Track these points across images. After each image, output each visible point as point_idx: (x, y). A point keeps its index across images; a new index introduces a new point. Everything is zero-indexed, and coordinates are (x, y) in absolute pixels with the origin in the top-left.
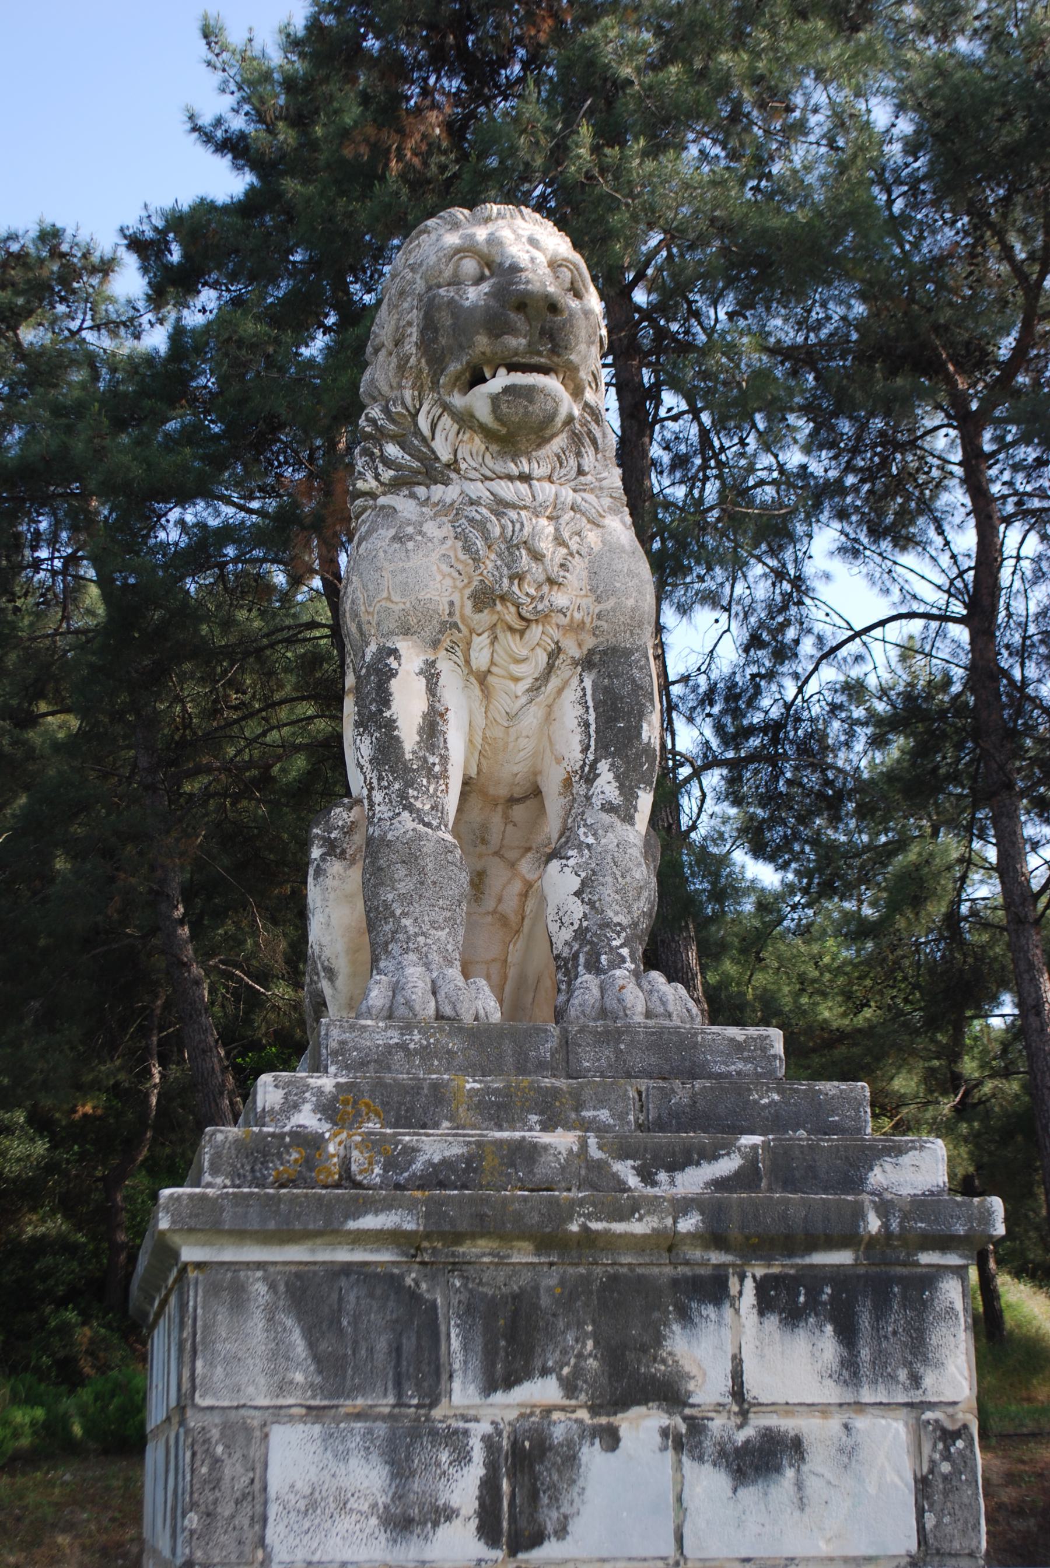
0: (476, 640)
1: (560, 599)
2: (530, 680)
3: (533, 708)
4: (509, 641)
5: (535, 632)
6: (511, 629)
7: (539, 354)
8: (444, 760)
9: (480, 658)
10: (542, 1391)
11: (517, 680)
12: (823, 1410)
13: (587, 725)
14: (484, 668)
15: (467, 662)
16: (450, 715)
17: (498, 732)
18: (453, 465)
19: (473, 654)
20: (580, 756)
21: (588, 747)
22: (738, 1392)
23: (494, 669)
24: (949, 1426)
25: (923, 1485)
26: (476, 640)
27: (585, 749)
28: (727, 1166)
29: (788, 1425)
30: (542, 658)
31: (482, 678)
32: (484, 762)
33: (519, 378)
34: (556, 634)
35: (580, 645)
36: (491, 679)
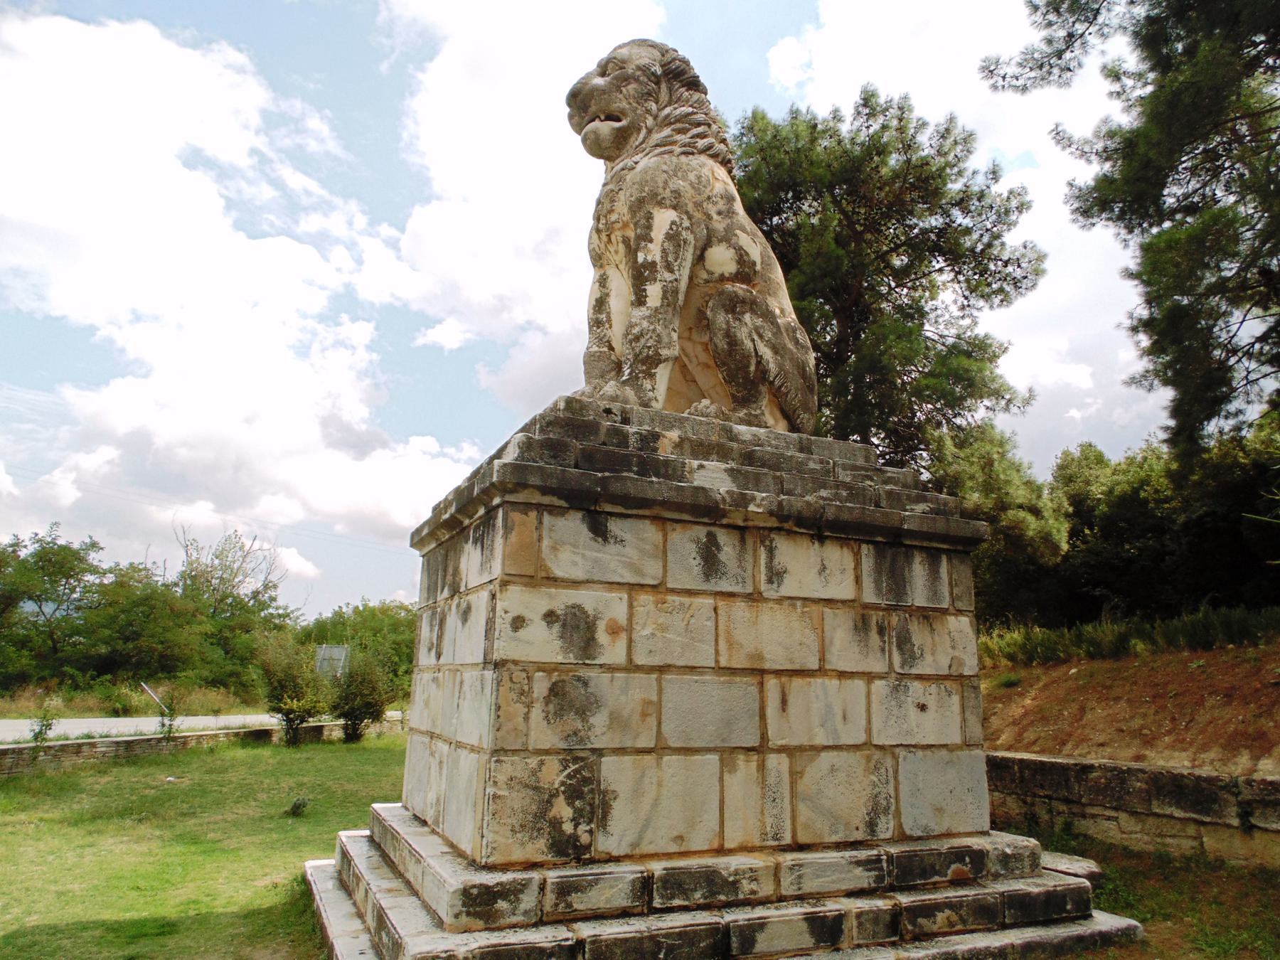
1: (613, 217)
5: (613, 237)
8: (608, 314)
16: (613, 294)
30: (621, 247)
34: (618, 233)
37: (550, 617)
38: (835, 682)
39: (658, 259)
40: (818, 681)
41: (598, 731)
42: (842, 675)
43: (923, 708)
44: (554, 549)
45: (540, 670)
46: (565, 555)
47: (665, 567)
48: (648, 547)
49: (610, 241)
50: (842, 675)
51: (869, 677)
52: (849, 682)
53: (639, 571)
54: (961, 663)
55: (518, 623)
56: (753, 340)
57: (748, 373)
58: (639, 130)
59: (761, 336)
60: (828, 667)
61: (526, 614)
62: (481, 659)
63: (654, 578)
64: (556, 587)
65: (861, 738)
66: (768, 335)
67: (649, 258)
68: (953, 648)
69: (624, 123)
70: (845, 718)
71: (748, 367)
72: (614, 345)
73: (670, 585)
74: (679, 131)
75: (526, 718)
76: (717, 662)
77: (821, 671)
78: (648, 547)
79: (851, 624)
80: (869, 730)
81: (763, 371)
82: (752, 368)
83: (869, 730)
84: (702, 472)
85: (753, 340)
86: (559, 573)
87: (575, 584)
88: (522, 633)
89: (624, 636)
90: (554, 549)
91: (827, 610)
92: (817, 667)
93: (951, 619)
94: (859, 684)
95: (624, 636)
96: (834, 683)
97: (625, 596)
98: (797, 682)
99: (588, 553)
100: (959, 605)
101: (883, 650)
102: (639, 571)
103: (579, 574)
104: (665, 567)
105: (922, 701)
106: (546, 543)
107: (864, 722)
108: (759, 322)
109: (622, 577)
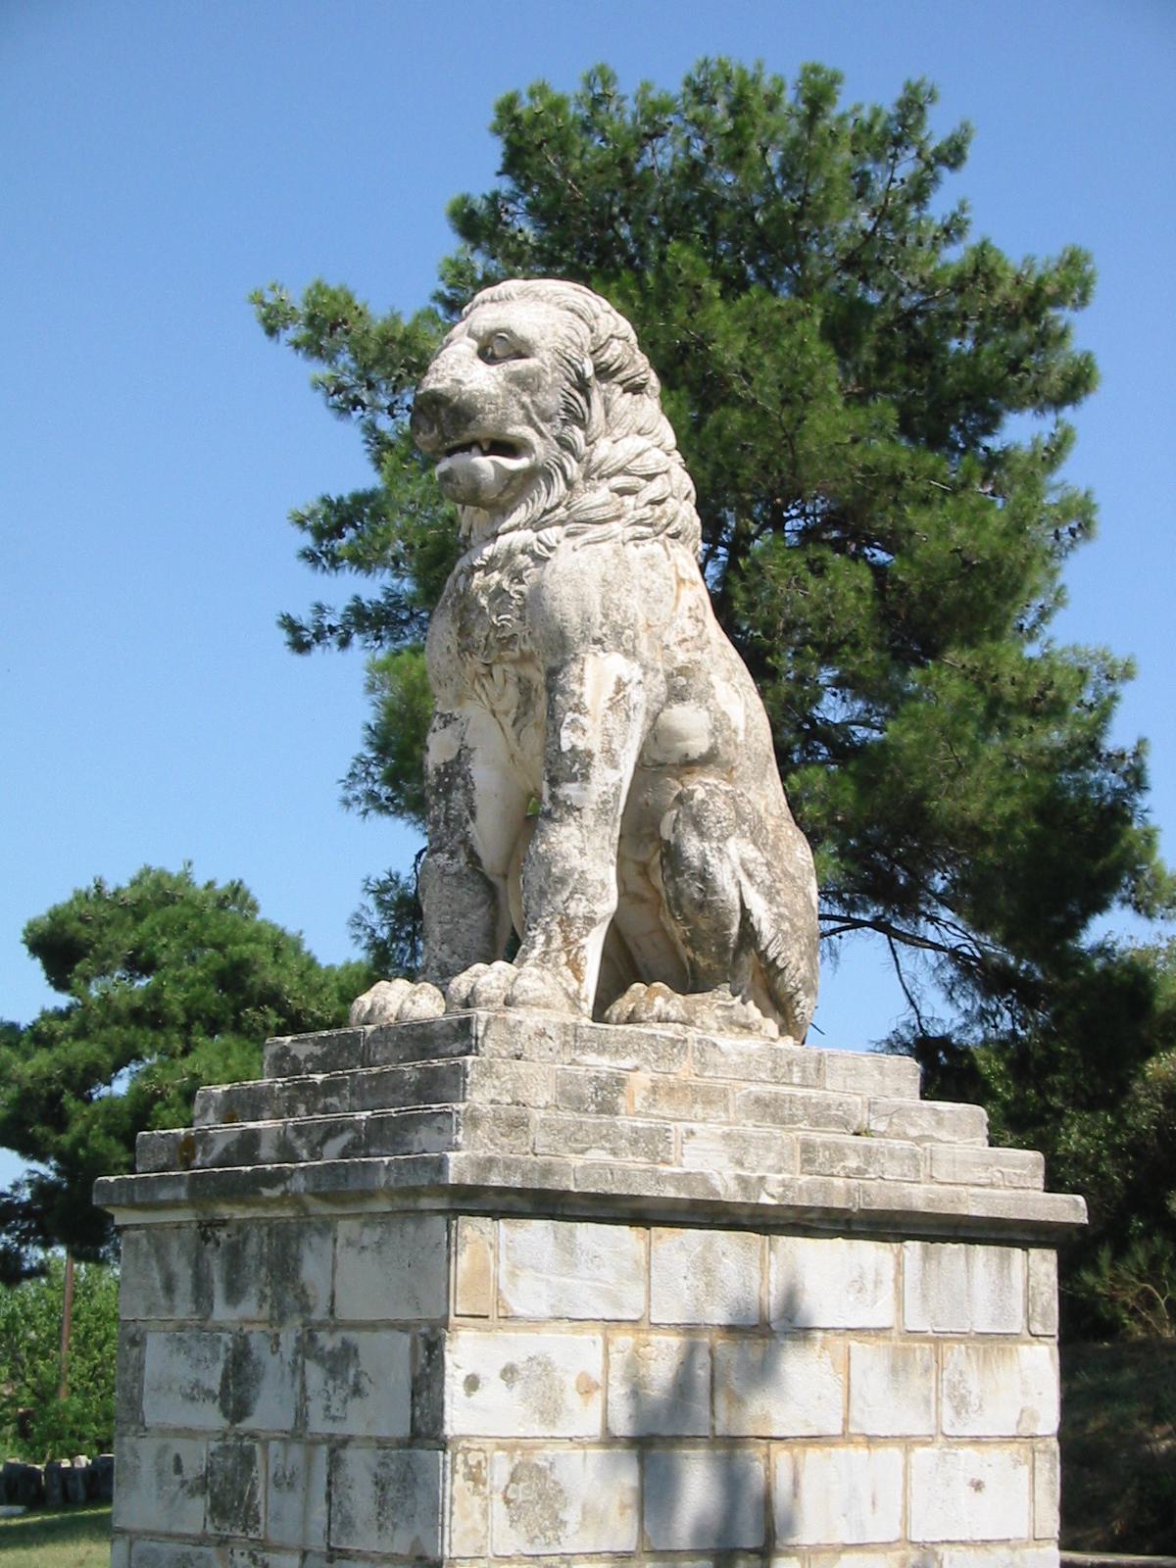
5: (497, 671)
10: (249, 1307)
12: (373, 1326)
16: (478, 755)
22: (332, 1312)
24: (433, 1339)
25: (415, 1381)
28: (346, 1137)
29: (353, 1336)
30: (512, 693)
34: (509, 668)
37: (509, 1373)
38: (863, 1451)
40: (841, 1451)
41: (571, 1528)
42: (871, 1440)
43: (978, 1486)
44: (513, 1275)
45: (499, 1447)
46: (527, 1281)
47: (649, 1291)
48: (625, 1264)
50: (871, 1440)
51: (907, 1442)
52: (881, 1451)
53: (617, 1303)
54: (1035, 1419)
55: (472, 1383)
56: (739, 884)
57: (727, 937)
58: (549, 477)
59: (750, 876)
60: (852, 1430)
61: (482, 1372)
62: (403, 1430)
63: (635, 1311)
64: (516, 1330)
65: (894, 1533)
66: (762, 873)
68: (1024, 1393)
70: (874, 1503)
71: (727, 928)
72: (481, 851)
73: (653, 1320)
74: (622, 492)
75: (485, 1514)
76: (713, 1428)
77: (845, 1438)
78: (625, 1264)
79: (886, 1362)
80: (905, 1522)
81: (749, 934)
82: (735, 930)
83: (905, 1522)
84: (692, 1142)
85: (739, 884)
86: (519, 1310)
87: (534, 1323)
88: (477, 1395)
89: (598, 1396)
90: (513, 1275)
91: (853, 1344)
92: (839, 1432)
93: (1024, 1349)
94: (895, 1453)
95: (598, 1396)
96: (861, 1452)
97: (599, 1338)
98: (813, 1454)
99: (552, 1278)
100: (1037, 1329)
101: (927, 1402)
102: (617, 1303)
103: (543, 1310)
104: (649, 1291)
105: (978, 1477)
106: (504, 1266)
107: (899, 1509)
108: (751, 852)
109: (596, 1310)
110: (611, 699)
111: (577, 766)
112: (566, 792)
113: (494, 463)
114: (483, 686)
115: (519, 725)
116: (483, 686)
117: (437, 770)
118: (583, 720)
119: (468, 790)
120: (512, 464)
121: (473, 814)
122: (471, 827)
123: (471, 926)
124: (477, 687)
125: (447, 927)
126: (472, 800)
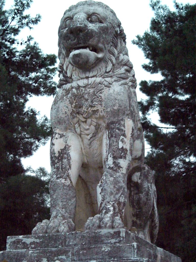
0: (76, 125)
2: (91, 134)
3: (95, 142)
4: (83, 125)
5: (89, 121)
6: (83, 122)
7: (80, 44)
9: (78, 130)
11: (88, 135)
13: (107, 144)
14: (79, 133)
15: (76, 132)
16: (72, 148)
17: (88, 150)
18: (71, 78)
19: (76, 130)
20: (106, 154)
21: (107, 151)
23: (82, 133)
26: (76, 125)
27: (106, 152)
30: (93, 128)
31: (80, 135)
32: (87, 158)
33: (77, 52)
34: (95, 120)
35: (104, 122)
36: (82, 136)
39: (128, 148)
49: (86, 122)
58: (106, 62)
67: (125, 147)
69: (100, 55)
110: (131, 134)
111: (123, 154)
112: (119, 162)
113: (95, 55)
114: (80, 125)
115: (91, 140)
116: (80, 125)
117: (59, 152)
118: (125, 139)
119: (69, 159)
120: (100, 55)
121: (70, 167)
122: (70, 171)
123: (72, 204)
124: (77, 125)
125: (64, 203)
126: (70, 163)
